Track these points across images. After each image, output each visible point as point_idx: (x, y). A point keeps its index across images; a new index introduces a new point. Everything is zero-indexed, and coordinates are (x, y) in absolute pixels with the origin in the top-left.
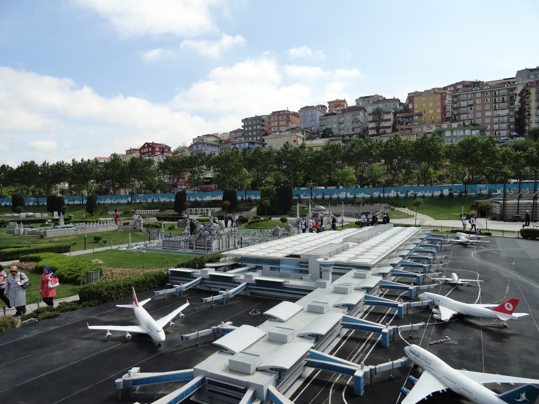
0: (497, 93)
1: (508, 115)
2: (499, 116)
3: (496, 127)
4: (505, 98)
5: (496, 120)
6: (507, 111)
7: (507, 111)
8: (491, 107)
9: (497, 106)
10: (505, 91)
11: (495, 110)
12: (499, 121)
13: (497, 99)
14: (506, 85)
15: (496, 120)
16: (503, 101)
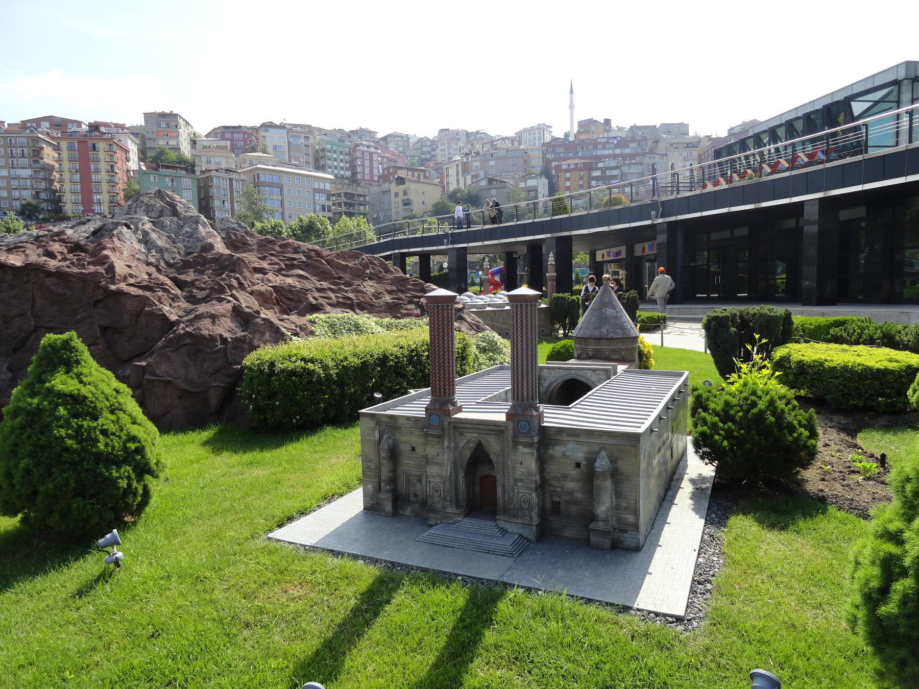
0: (13, 141)
1: (31, 177)
2: (18, 178)
3: (16, 194)
4: (26, 150)
5: (15, 183)
6: (28, 172)
7: (28, 172)
8: (7, 161)
9: (15, 162)
10: (24, 140)
11: (13, 167)
12: (19, 185)
13: (14, 152)
14: (28, 131)
15: (15, 183)
16: (23, 156)
